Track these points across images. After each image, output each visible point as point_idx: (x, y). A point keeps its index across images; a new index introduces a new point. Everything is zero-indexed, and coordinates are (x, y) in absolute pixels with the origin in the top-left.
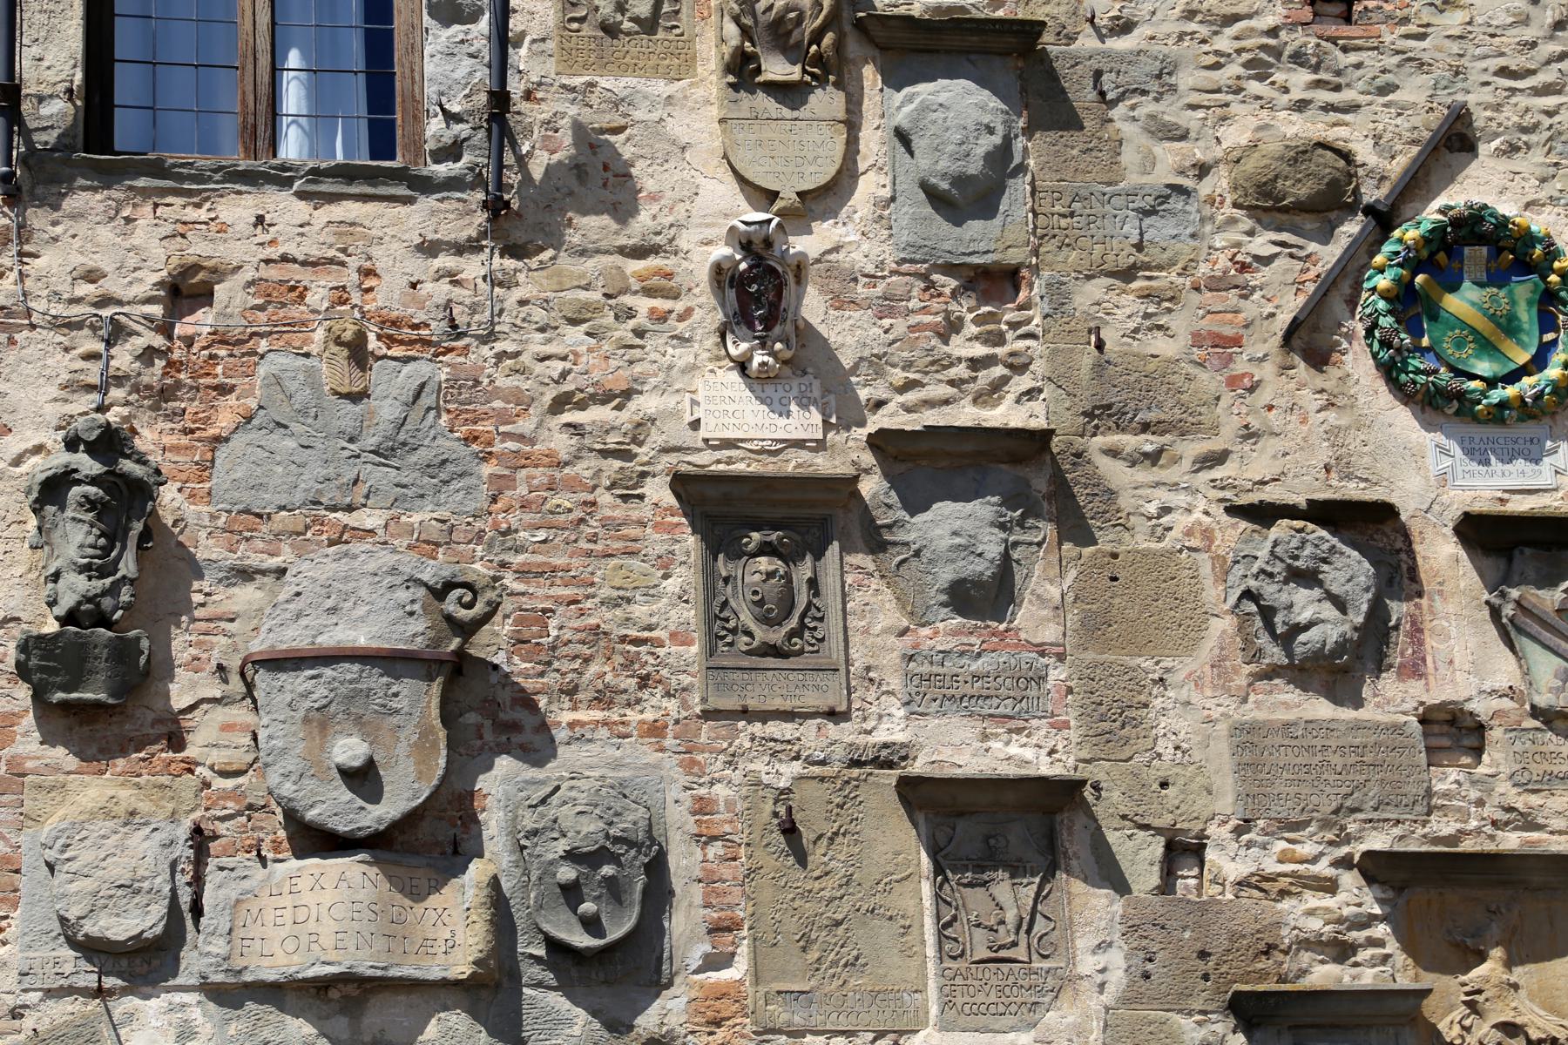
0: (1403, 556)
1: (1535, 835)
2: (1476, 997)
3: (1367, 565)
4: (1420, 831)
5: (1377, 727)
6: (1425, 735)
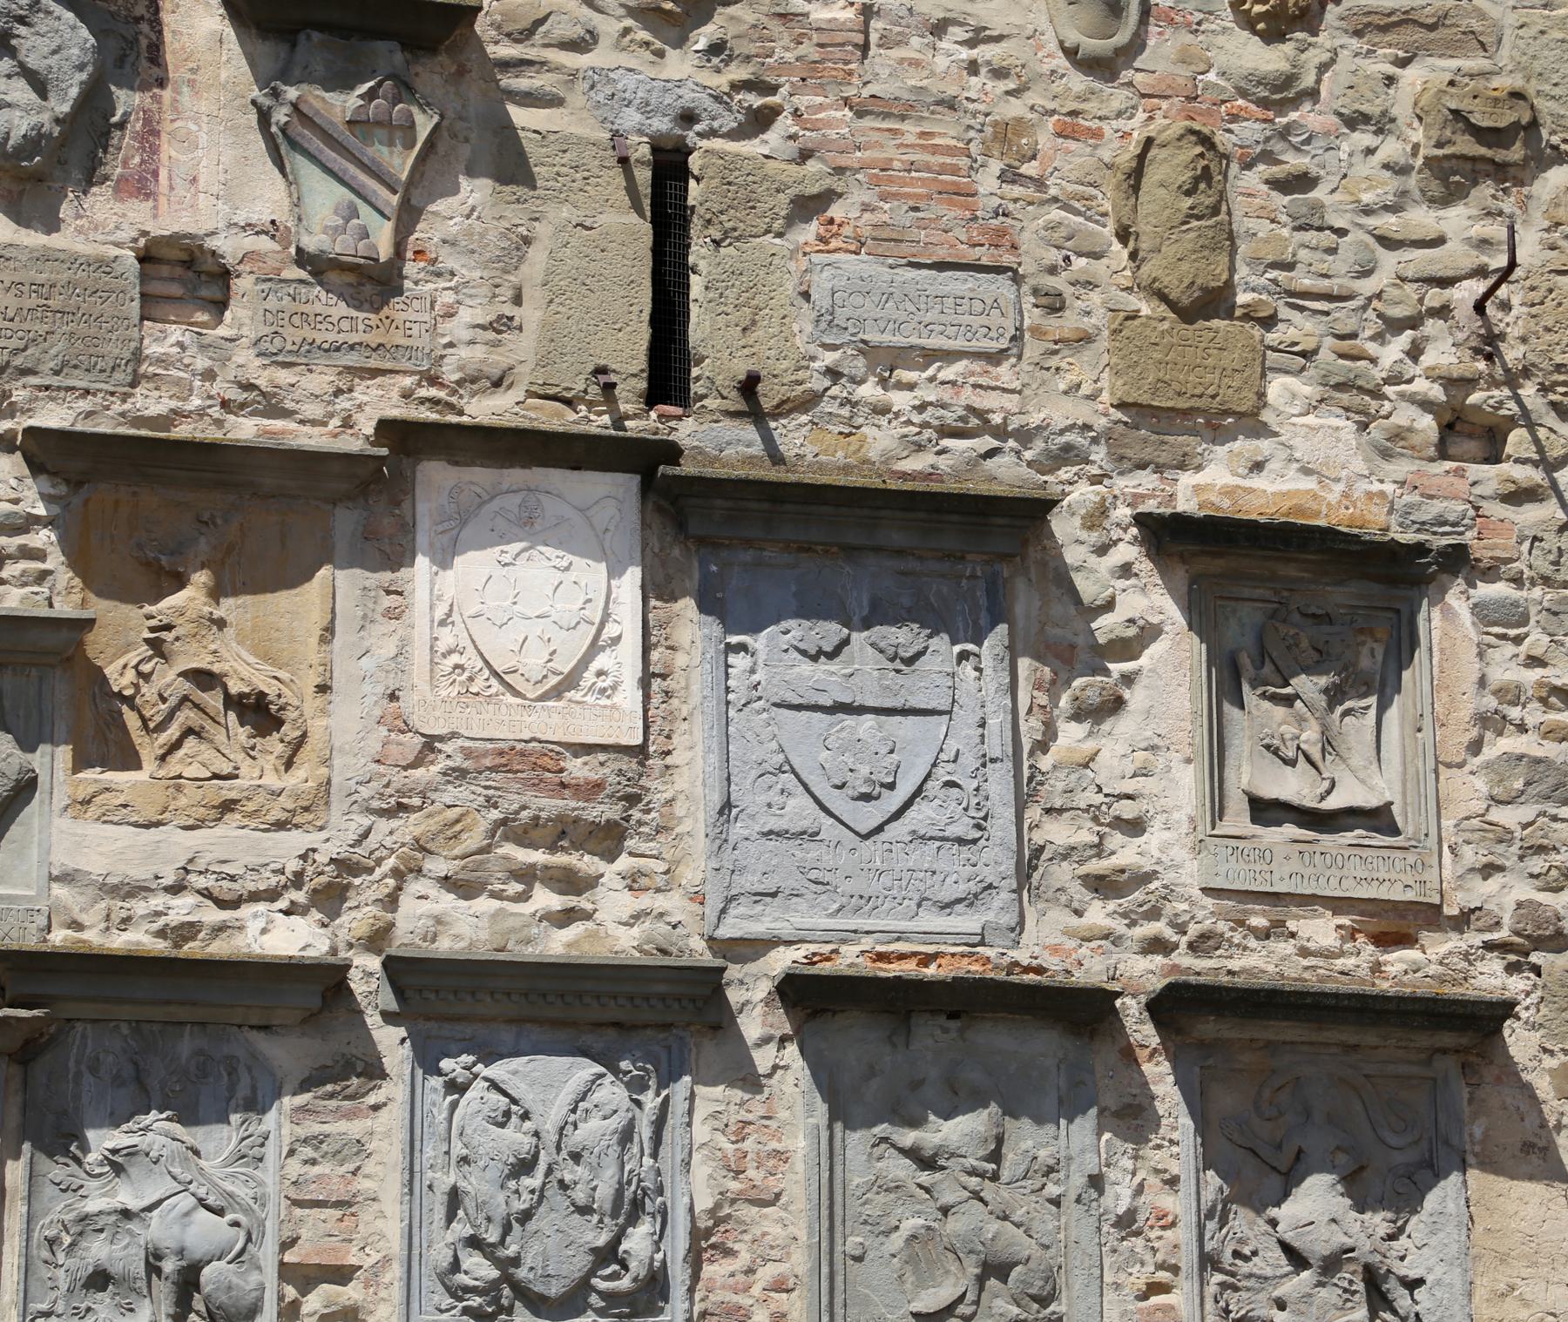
0: (144, 27)
1: (278, 424)
2: (163, 635)
3: (84, 32)
4: (118, 407)
5: (74, 260)
6: (144, 277)
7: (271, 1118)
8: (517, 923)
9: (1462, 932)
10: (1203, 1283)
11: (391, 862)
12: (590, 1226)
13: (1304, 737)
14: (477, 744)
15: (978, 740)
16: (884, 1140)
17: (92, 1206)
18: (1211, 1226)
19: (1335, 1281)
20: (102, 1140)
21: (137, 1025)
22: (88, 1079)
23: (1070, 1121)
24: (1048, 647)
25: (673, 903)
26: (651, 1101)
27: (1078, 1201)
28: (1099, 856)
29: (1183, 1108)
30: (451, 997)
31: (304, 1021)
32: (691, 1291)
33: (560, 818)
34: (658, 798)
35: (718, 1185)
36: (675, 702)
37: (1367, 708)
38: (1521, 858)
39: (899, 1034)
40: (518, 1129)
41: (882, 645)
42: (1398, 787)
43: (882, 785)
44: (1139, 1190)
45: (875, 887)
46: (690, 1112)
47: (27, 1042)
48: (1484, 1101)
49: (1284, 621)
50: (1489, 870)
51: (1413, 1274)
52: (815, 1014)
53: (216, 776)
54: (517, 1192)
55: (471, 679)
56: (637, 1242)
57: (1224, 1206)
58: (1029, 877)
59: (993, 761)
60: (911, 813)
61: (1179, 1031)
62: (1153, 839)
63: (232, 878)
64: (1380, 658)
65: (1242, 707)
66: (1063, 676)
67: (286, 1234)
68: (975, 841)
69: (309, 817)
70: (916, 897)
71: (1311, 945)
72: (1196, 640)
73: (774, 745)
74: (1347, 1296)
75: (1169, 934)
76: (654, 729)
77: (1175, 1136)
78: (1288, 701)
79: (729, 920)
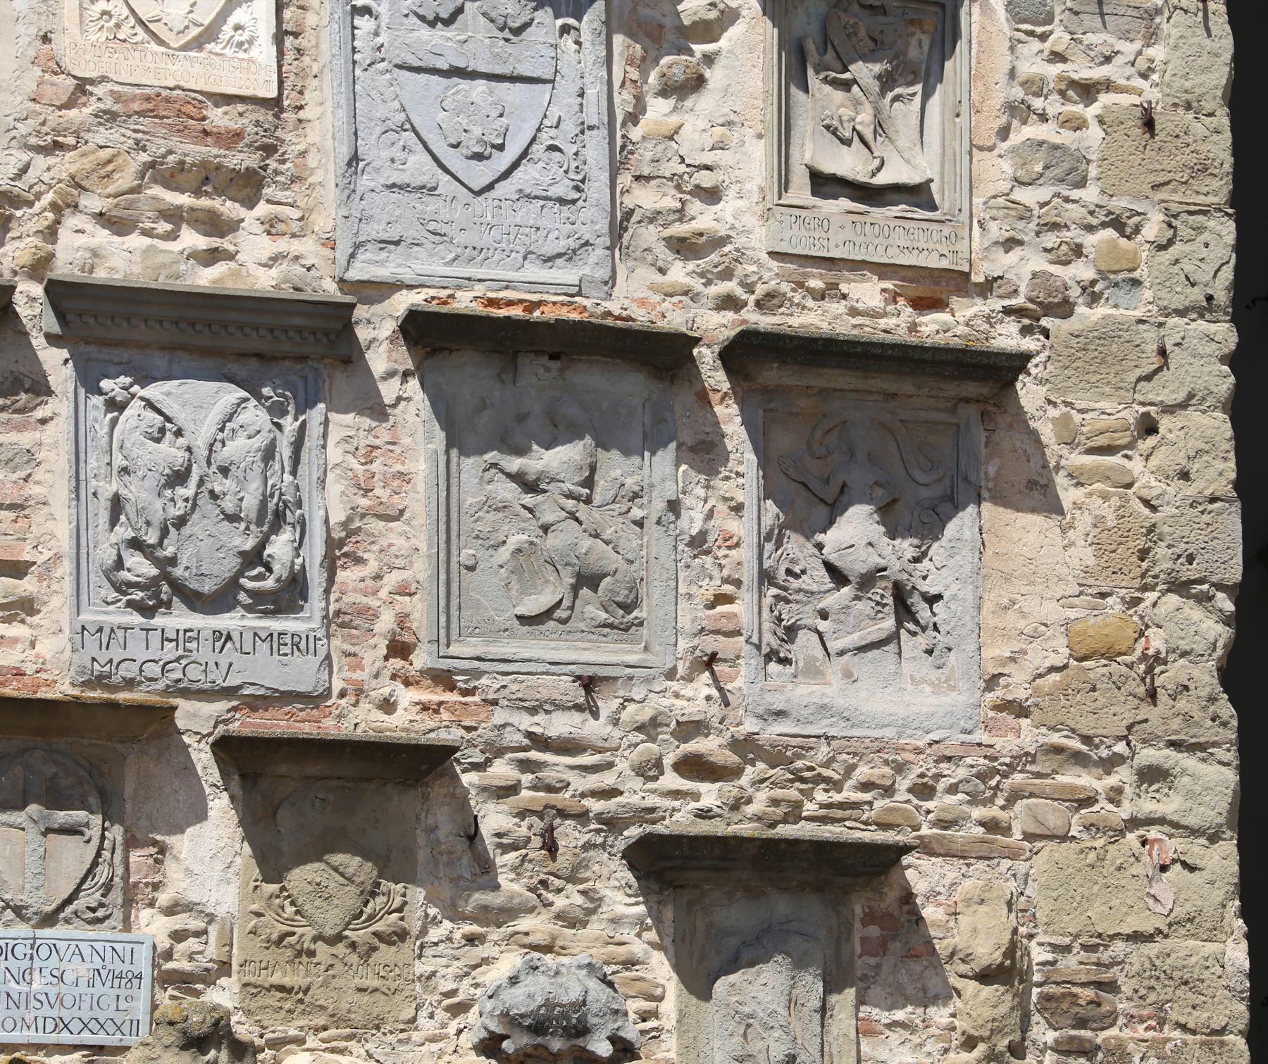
8: (166, 259)
9: (986, 298)
10: (761, 595)
11: (49, 197)
12: (238, 532)
13: (859, 119)
14: (126, 89)
15: (577, 109)
16: (494, 465)
18: (769, 547)
19: (869, 595)
23: (653, 453)
24: (639, 26)
25: (308, 248)
26: (290, 424)
27: (658, 523)
28: (681, 220)
29: (748, 445)
30: (109, 322)
32: (327, 592)
33: (204, 164)
34: (292, 150)
35: (349, 502)
36: (306, 59)
37: (914, 94)
38: (1038, 234)
39: (506, 368)
40: (172, 444)
41: (493, 14)
42: (937, 168)
43: (493, 146)
44: (710, 515)
45: (486, 240)
46: (325, 436)
48: (998, 444)
49: (845, 11)
50: (1011, 243)
51: (933, 591)
52: (434, 352)
54: (172, 500)
55: (118, 26)
56: (280, 547)
57: (780, 531)
58: (621, 237)
59: (591, 128)
60: (518, 174)
61: (747, 378)
62: (728, 207)
64: (926, 48)
65: (807, 91)
66: (653, 53)
68: (574, 202)
70: (522, 250)
71: (860, 306)
72: (769, 24)
73: (396, 105)
74: (879, 608)
75: (740, 292)
76: (288, 84)
77: (741, 469)
78: (846, 86)
79: (357, 264)
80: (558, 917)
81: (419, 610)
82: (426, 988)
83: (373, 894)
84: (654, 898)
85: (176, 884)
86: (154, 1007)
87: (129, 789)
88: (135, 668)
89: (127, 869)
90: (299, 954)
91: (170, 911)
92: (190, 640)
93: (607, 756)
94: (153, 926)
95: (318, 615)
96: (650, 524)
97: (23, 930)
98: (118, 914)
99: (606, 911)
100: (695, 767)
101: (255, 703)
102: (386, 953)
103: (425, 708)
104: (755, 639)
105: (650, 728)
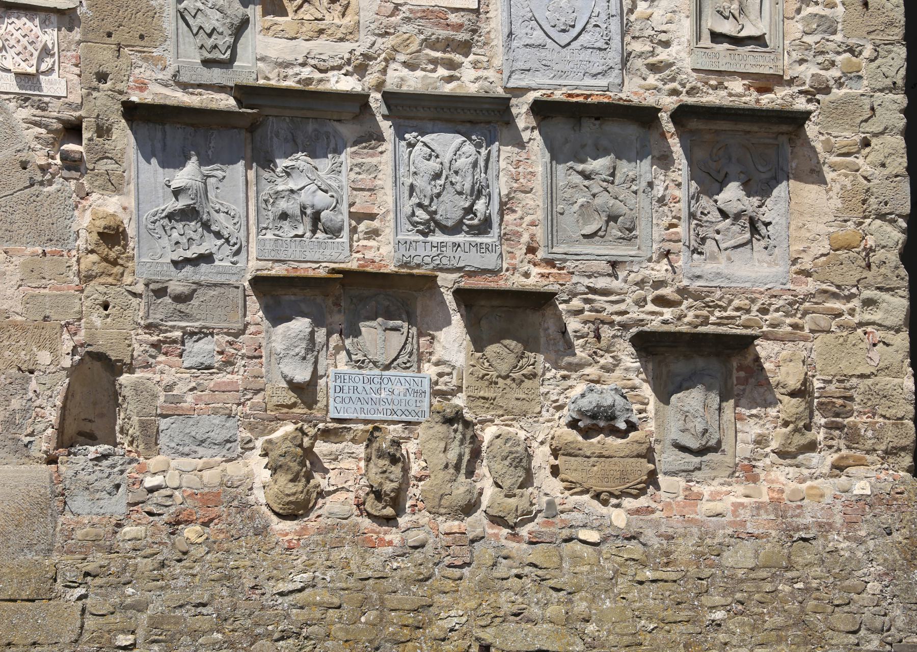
7: (343, 155)
10: (689, 224)
11: (383, 55)
16: (571, 168)
17: (280, 188)
18: (693, 202)
20: (282, 163)
21: (292, 118)
22: (275, 139)
23: (641, 161)
25: (491, 74)
26: (484, 152)
27: (644, 192)
28: (652, 56)
31: (354, 118)
32: (500, 225)
33: (447, 39)
38: (814, 56)
40: (435, 161)
42: (768, 28)
44: (666, 188)
45: (567, 68)
46: (499, 156)
47: (252, 124)
50: (802, 61)
51: (767, 220)
53: (316, 19)
56: (480, 206)
59: (613, 16)
60: (581, 38)
61: (683, 126)
62: (674, 49)
63: (324, 61)
67: (351, 201)
68: (605, 49)
69: (352, 36)
71: (733, 92)
73: (528, 9)
75: (679, 87)
77: (680, 167)
79: (512, 80)
80: (602, 368)
81: (540, 233)
82: (545, 399)
83: (522, 358)
84: (644, 359)
85: (439, 352)
86: (431, 405)
87: (418, 312)
88: (420, 258)
89: (419, 346)
90: (491, 383)
91: (437, 364)
92: (443, 246)
93: (622, 297)
94: (429, 370)
95: (496, 235)
96: (640, 193)
97: (377, 371)
98: (415, 365)
99: (623, 365)
100: (661, 301)
101: (471, 274)
102: (527, 383)
103: (543, 276)
104: (687, 244)
105: (641, 284)
